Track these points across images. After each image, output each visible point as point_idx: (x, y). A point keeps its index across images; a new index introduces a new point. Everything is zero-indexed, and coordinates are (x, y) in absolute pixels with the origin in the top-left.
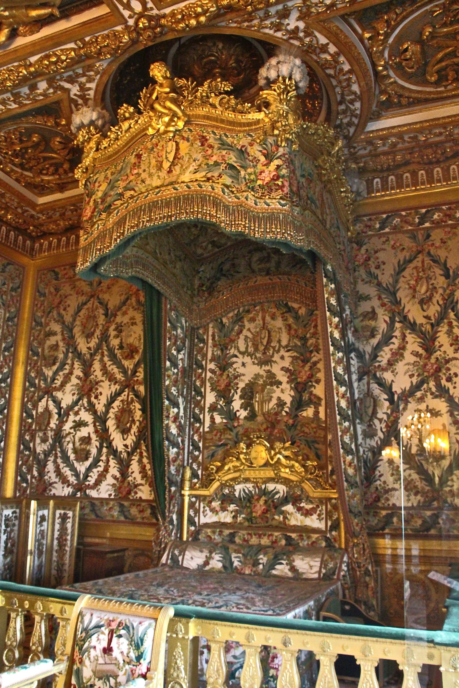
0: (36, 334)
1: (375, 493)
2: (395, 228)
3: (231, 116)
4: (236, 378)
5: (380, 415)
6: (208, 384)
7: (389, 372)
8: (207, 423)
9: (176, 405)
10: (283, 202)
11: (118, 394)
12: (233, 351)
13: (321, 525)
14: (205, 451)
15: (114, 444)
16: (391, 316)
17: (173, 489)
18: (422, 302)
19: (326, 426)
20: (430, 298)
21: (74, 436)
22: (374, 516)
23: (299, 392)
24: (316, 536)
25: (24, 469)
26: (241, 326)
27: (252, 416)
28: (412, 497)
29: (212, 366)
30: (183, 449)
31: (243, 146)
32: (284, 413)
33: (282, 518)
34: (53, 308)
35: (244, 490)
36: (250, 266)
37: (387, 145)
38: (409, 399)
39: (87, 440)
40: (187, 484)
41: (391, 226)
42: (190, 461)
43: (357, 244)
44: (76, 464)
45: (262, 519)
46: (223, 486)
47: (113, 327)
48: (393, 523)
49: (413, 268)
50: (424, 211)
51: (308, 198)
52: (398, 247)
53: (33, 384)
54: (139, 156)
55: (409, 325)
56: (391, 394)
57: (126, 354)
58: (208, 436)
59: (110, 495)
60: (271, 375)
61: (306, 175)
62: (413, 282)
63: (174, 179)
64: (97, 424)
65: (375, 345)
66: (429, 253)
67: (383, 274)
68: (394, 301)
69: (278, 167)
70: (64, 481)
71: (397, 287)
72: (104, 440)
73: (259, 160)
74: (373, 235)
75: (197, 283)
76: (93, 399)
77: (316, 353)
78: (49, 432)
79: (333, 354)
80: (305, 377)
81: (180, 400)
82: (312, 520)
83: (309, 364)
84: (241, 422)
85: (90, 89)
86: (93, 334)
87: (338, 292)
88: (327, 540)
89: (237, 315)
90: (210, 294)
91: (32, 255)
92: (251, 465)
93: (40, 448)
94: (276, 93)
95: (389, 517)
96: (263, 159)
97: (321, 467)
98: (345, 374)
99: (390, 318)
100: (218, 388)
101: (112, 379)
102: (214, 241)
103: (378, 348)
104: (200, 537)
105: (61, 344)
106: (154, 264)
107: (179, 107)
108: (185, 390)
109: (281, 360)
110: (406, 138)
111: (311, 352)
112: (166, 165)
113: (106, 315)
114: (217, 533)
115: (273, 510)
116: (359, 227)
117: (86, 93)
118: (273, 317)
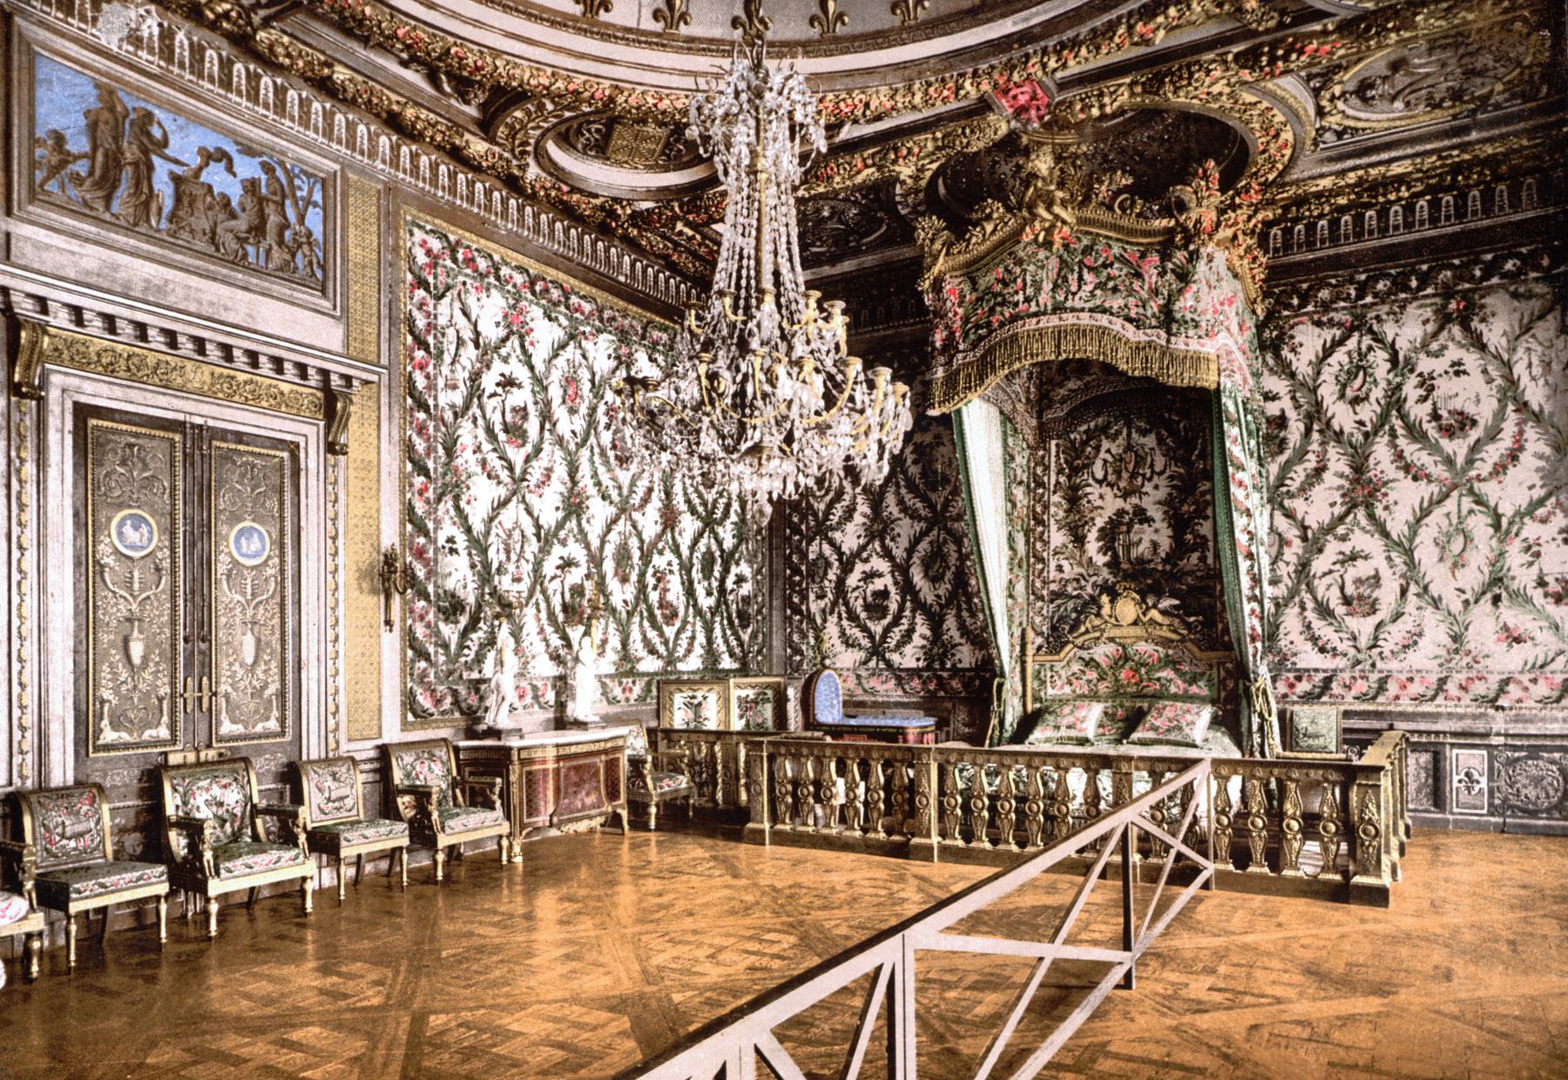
11: (924, 534)
29: (1056, 498)
39: (884, 594)
76: (887, 541)
101: (914, 515)
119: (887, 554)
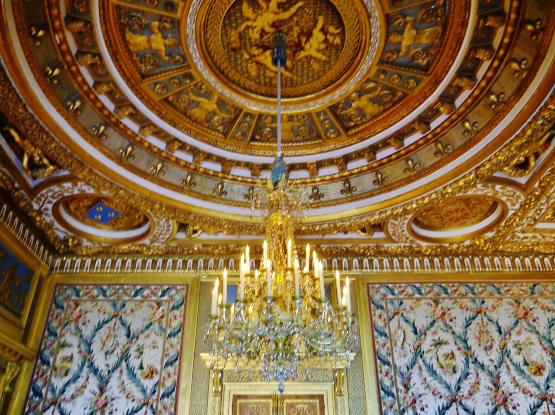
18: (107, 353)
20: (113, 351)
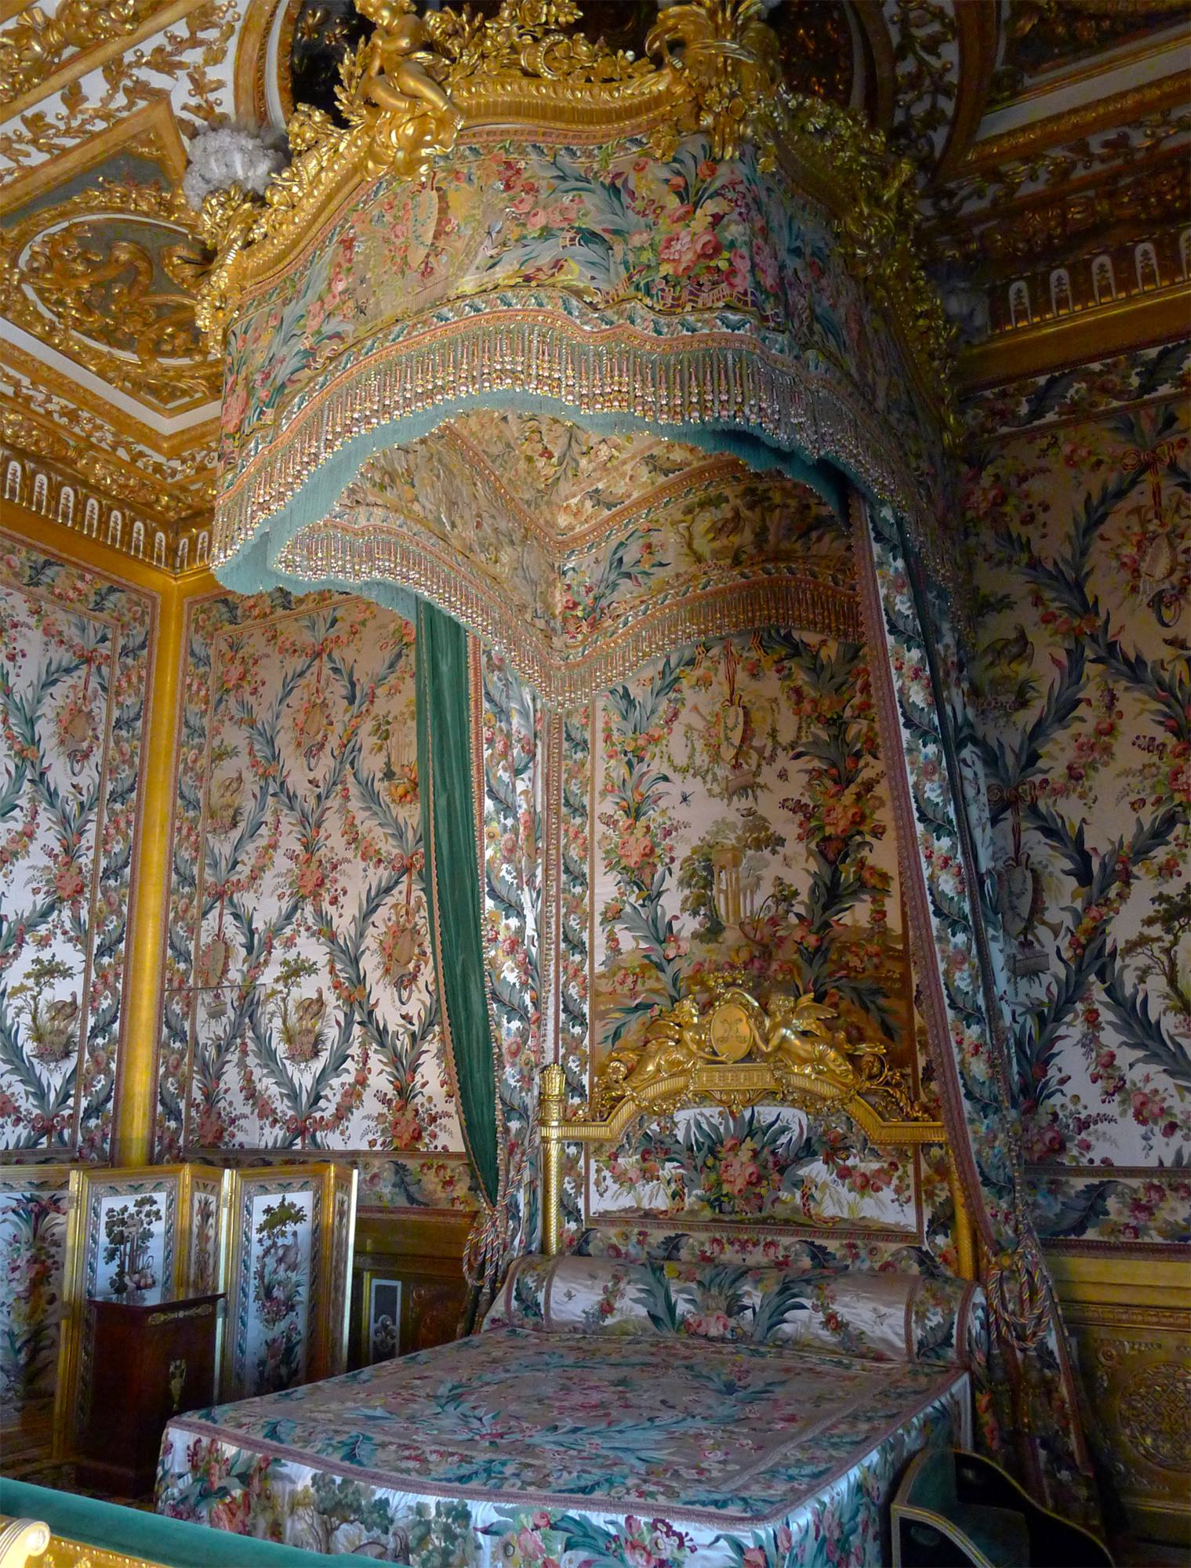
0: (191, 756)
1: (1050, 1127)
2: (1074, 408)
3: (581, 96)
4: (668, 833)
5: (1053, 915)
6: (599, 854)
7: (1074, 796)
8: (600, 956)
9: (513, 908)
10: (733, 317)
12: (658, 767)
13: (906, 1217)
14: (598, 1025)
15: (378, 1013)
16: (1072, 646)
17: (514, 1125)
18: (1158, 602)
19: (906, 950)
21: (284, 1000)
22: (1051, 1192)
23: (831, 863)
24: (893, 1247)
25: (171, 1086)
26: (676, 700)
27: (713, 931)
28: (1158, 1140)
29: (607, 806)
30: (539, 1022)
31: (618, 175)
32: (793, 920)
33: (798, 1201)
34: (227, 691)
35: (698, 1125)
36: (690, 545)
37: (1043, 176)
38: (1135, 870)
39: (315, 1007)
40: (555, 1111)
41: (1061, 405)
42: (562, 1051)
43: (969, 461)
44: (290, 1069)
45: (747, 1200)
46: (642, 1115)
47: (368, 726)
48: (1107, 1213)
49: (1129, 513)
50: (1153, 352)
51: (814, 317)
52: (1084, 460)
53: (187, 880)
54: (348, 244)
55: (1124, 668)
56: (1082, 858)
57: (401, 791)
58: (604, 986)
59: (372, 1143)
60: (756, 823)
61: (808, 251)
62: (1129, 551)
63: (438, 291)
64: (338, 966)
65: (1029, 729)
66: (1173, 468)
67: (1044, 536)
68: (1079, 609)
69: (717, 219)
70: (265, 1111)
71: (1086, 570)
72: (356, 1005)
73: (662, 208)
74: (1011, 435)
75: (559, 600)
77: (868, 758)
78: (227, 991)
79: (910, 750)
80: (843, 824)
81: (526, 897)
82: (880, 1204)
83: (853, 788)
84: (685, 946)
85: (220, 84)
86: (322, 746)
87: (916, 580)
88: (923, 1258)
89: (663, 673)
90: (593, 626)
91: (174, 567)
92: (713, 1059)
93: (208, 1031)
94: (703, 11)
95: (1097, 1194)
96: (673, 202)
97: (899, 1060)
98: (946, 803)
99: (1069, 652)
100: (624, 862)
102: (597, 491)
103: (1038, 731)
104: (591, 1249)
105: (248, 776)
106: (435, 550)
107: (440, 86)
108: (539, 872)
109: (779, 782)
110: (1095, 146)
111: (858, 755)
112: (417, 257)
113: (351, 699)
114: (634, 1239)
115: (776, 1176)
116: (973, 416)
117: (211, 97)
118: (755, 673)
119: (326, 932)
